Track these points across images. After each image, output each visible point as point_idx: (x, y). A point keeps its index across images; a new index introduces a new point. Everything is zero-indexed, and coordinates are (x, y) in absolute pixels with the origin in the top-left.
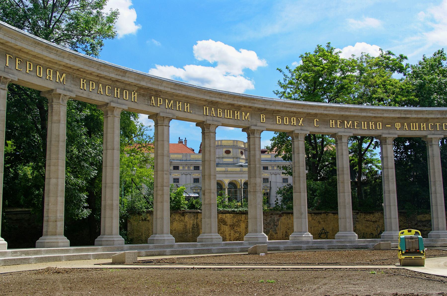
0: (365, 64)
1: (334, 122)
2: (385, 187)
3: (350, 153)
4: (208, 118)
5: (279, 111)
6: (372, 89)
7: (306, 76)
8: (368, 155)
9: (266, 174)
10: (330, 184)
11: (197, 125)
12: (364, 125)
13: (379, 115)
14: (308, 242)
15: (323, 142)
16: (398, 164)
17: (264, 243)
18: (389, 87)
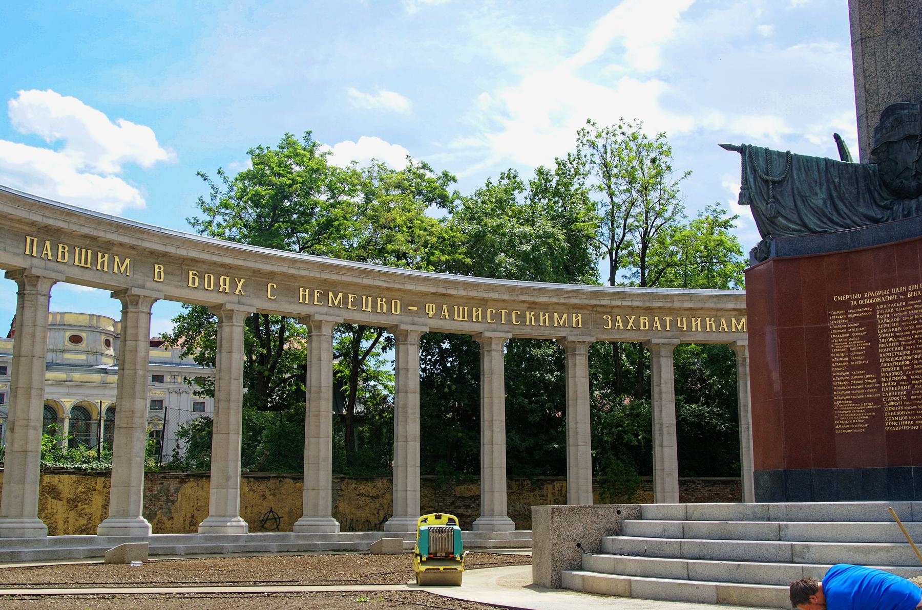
0: (376, 183)
1: (307, 293)
2: (399, 429)
3: (335, 357)
4: (36, 262)
5: (194, 261)
6: (386, 232)
7: (257, 194)
8: (371, 363)
9: (157, 392)
10: (290, 418)
11: (113, 295)
12: (367, 303)
13: (397, 286)
14: (237, 538)
15: (282, 330)
16: (426, 384)
17: (142, 539)
18: (418, 232)
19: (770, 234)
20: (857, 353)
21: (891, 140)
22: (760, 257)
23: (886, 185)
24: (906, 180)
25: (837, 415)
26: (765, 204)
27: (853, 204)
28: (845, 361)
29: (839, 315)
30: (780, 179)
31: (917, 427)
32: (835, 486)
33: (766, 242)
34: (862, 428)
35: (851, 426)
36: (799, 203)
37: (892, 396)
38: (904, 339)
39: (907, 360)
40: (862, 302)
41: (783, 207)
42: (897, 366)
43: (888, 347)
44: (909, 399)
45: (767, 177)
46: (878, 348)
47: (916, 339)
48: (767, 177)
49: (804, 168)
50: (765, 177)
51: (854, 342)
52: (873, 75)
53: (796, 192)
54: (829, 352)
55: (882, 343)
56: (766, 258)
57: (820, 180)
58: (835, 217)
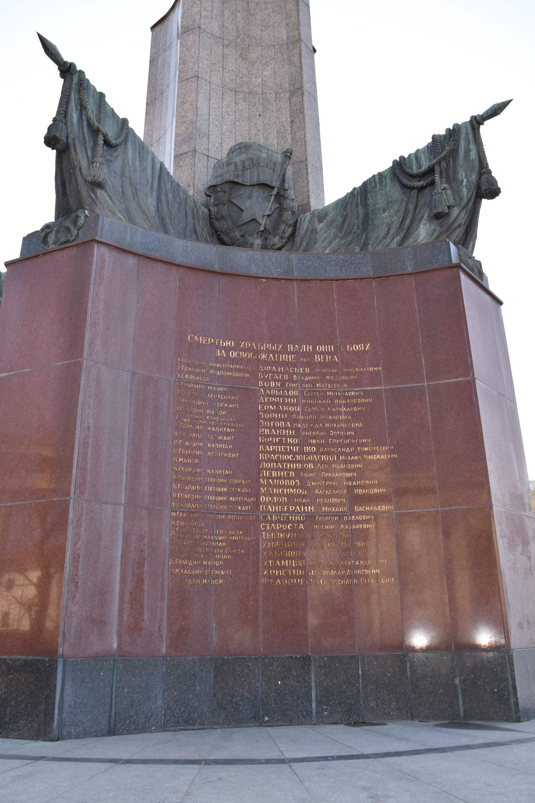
42: (291, 470)
47: (328, 430)
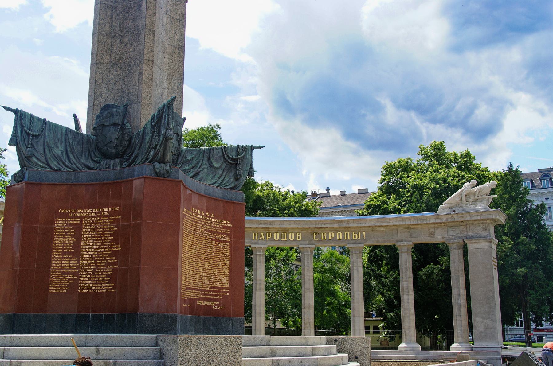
19: (26, 167)
20: (69, 245)
21: (105, 124)
22: (18, 180)
23: (98, 149)
24: (110, 148)
25: (51, 281)
26: (25, 148)
27: (79, 157)
28: (61, 249)
29: (61, 221)
30: (37, 134)
31: (96, 291)
32: (44, 324)
33: (23, 171)
34: (65, 290)
35: (58, 288)
36: (47, 150)
37: (85, 272)
38: (96, 239)
39: (96, 251)
40: (76, 215)
41: (36, 151)
42: (90, 254)
43: (87, 243)
44: (94, 274)
45: (29, 132)
46: (81, 243)
47: (103, 240)
48: (29, 132)
49: (53, 131)
50: (28, 131)
51: (68, 238)
52: (100, 85)
53: (46, 144)
54: (52, 243)
55: (83, 240)
56: (21, 181)
57: (61, 139)
58: (67, 163)
